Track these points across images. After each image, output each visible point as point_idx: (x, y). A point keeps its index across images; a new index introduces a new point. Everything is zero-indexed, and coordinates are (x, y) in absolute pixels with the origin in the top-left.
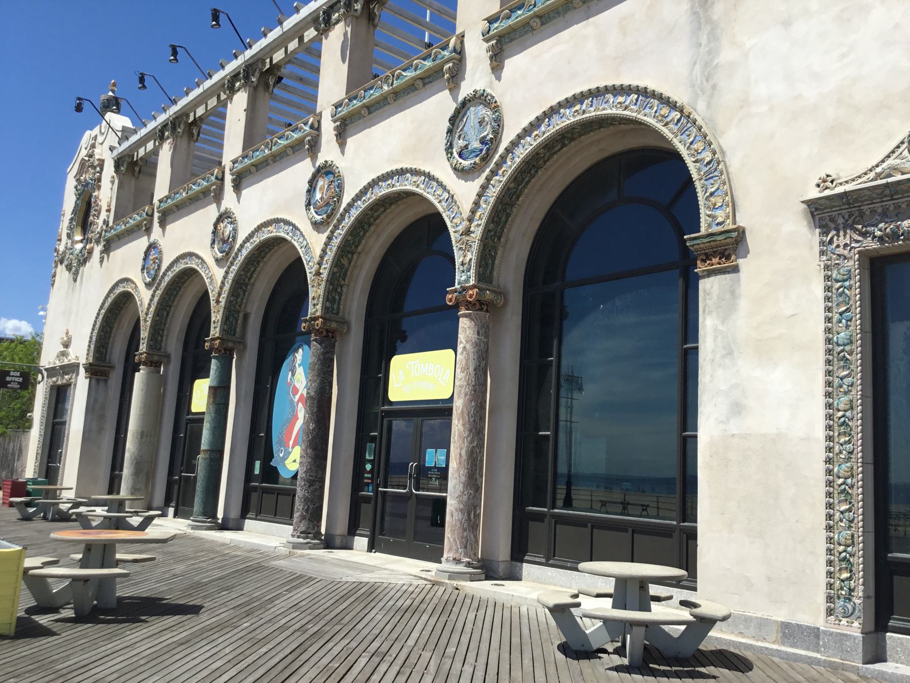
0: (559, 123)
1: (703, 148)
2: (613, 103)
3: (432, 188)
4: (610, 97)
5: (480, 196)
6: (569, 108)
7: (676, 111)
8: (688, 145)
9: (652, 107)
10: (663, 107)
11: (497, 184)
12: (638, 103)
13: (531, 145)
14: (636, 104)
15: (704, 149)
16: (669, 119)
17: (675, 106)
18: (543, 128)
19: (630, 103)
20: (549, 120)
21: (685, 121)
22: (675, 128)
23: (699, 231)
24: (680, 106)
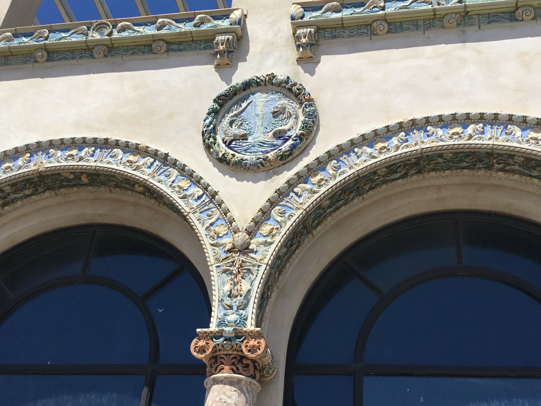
1: (225, 233)
2: (121, 159)
6: (62, 150)
7: (199, 187)
8: (208, 225)
9: (169, 175)
10: (183, 179)
12: (152, 168)
15: (227, 234)
17: (199, 182)
18: (20, 162)
20: (32, 156)
21: (207, 200)
22: (195, 204)
23: (208, 327)
24: (204, 183)
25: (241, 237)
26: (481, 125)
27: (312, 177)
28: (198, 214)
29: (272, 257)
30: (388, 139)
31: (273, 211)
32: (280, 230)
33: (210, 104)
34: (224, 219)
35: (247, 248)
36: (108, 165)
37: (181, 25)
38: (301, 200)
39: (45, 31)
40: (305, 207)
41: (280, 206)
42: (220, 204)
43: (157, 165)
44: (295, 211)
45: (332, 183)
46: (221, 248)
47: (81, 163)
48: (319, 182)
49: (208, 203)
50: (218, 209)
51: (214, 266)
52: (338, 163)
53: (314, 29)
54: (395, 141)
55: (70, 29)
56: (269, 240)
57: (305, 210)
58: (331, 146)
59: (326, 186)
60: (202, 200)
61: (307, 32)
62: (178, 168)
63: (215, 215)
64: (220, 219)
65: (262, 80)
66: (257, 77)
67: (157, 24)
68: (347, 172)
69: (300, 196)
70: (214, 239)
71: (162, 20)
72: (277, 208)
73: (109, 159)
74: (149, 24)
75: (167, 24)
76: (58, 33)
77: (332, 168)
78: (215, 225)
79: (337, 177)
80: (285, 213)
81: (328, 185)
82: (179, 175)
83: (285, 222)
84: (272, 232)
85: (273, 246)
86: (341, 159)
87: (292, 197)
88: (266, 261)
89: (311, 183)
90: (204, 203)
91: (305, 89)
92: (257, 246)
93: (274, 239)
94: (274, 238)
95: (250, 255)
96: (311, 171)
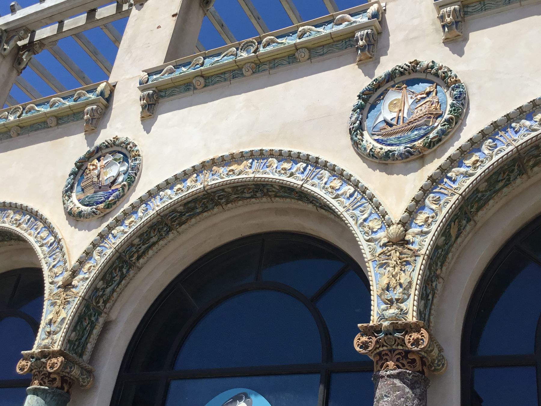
1: (379, 227)
2: (276, 168)
3: (36, 229)
4: (274, 161)
5: (94, 245)
6: (223, 167)
11: (119, 235)
12: (306, 173)
13: (171, 199)
15: (380, 229)
17: (349, 180)
18: (189, 183)
19: (297, 171)
20: (198, 175)
21: (360, 196)
24: (355, 180)
25: (395, 230)
27: (466, 160)
29: (430, 247)
31: (427, 200)
32: (435, 219)
33: (356, 101)
34: (376, 213)
36: (265, 175)
37: (320, 29)
38: (455, 186)
39: (200, 58)
40: (460, 192)
41: (434, 193)
42: (371, 199)
43: (310, 170)
44: (450, 198)
45: (488, 164)
46: (377, 242)
49: (359, 200)
50: (370, 203)
51: (370, 262)
52: (494, 141)
53: (459, 6)
55: (221, 53)
56: (425, 229)
57: (461, 195)
58: (485, 124)
59: (482, 167)
60: (354, 198)
61: (364, 34)
62: (329, 169)
63: (368, 209)
64: (372, 213)
65: (405, 69)
66: (400, 67)
67: (298, 33)
68: (505, 150)
69: (454, 181)
70: (368, 234)
71: (303, 28)
74: (291, 35)
75: (308, 31)
76: (211, 59)
77: (487, 148)
79: (494, 157)
80: (440, 200)
81: (484, 166)
82: (331, 175)
83: (441, 210)
84: (427, 221)
85: (430, 236)
87: (446, 182)
88: (423, 251)
89: (466, 165)
90: (356, 200)
91: (451, 71)
92: (413, 237)
93: (430, 229)
94: (430, 227)
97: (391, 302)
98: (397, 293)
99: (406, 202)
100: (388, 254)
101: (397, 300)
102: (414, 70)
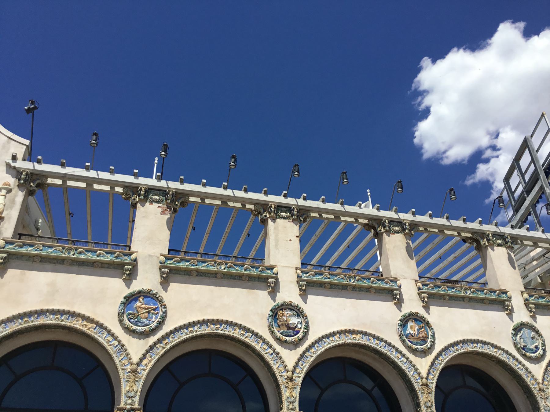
0: (42, 321)
8: (120, 359)
9: (103, 334)
10: (109, 336)
14: (94, 329)
16: (112, 343)
26: (226, 325)
27: (164, 341)
28: (116, 354)
30: (193, 326)
35: (136, 371)
37: (109, 256)
38: (158, 351)
43: (98, 328)
47: (62, 323)
48: (166, 343)
54: (196, 328)
57: (160, 356)
58: (172, 328)
60: (118, 347)
72: (149, 354)
73: (75, 322)
78: (123, 359)
86: (175, 334)
95: (138, 374)
96: (163, 338)
97: (130, 397)
98: (132, 394)
99: (140, 355)
100: (130, 376)
101: (132, 397)
102: (149, 293)
